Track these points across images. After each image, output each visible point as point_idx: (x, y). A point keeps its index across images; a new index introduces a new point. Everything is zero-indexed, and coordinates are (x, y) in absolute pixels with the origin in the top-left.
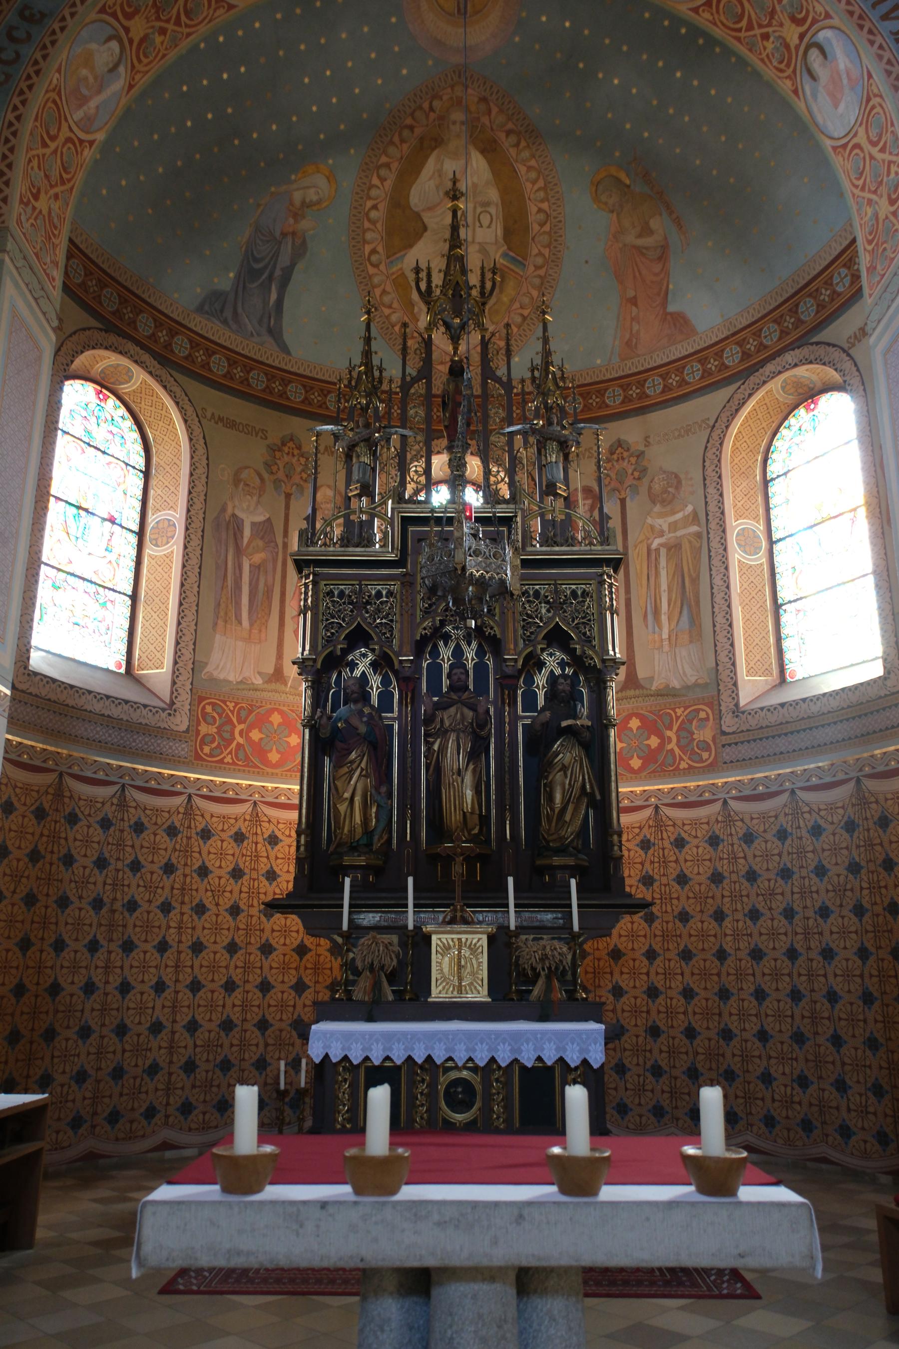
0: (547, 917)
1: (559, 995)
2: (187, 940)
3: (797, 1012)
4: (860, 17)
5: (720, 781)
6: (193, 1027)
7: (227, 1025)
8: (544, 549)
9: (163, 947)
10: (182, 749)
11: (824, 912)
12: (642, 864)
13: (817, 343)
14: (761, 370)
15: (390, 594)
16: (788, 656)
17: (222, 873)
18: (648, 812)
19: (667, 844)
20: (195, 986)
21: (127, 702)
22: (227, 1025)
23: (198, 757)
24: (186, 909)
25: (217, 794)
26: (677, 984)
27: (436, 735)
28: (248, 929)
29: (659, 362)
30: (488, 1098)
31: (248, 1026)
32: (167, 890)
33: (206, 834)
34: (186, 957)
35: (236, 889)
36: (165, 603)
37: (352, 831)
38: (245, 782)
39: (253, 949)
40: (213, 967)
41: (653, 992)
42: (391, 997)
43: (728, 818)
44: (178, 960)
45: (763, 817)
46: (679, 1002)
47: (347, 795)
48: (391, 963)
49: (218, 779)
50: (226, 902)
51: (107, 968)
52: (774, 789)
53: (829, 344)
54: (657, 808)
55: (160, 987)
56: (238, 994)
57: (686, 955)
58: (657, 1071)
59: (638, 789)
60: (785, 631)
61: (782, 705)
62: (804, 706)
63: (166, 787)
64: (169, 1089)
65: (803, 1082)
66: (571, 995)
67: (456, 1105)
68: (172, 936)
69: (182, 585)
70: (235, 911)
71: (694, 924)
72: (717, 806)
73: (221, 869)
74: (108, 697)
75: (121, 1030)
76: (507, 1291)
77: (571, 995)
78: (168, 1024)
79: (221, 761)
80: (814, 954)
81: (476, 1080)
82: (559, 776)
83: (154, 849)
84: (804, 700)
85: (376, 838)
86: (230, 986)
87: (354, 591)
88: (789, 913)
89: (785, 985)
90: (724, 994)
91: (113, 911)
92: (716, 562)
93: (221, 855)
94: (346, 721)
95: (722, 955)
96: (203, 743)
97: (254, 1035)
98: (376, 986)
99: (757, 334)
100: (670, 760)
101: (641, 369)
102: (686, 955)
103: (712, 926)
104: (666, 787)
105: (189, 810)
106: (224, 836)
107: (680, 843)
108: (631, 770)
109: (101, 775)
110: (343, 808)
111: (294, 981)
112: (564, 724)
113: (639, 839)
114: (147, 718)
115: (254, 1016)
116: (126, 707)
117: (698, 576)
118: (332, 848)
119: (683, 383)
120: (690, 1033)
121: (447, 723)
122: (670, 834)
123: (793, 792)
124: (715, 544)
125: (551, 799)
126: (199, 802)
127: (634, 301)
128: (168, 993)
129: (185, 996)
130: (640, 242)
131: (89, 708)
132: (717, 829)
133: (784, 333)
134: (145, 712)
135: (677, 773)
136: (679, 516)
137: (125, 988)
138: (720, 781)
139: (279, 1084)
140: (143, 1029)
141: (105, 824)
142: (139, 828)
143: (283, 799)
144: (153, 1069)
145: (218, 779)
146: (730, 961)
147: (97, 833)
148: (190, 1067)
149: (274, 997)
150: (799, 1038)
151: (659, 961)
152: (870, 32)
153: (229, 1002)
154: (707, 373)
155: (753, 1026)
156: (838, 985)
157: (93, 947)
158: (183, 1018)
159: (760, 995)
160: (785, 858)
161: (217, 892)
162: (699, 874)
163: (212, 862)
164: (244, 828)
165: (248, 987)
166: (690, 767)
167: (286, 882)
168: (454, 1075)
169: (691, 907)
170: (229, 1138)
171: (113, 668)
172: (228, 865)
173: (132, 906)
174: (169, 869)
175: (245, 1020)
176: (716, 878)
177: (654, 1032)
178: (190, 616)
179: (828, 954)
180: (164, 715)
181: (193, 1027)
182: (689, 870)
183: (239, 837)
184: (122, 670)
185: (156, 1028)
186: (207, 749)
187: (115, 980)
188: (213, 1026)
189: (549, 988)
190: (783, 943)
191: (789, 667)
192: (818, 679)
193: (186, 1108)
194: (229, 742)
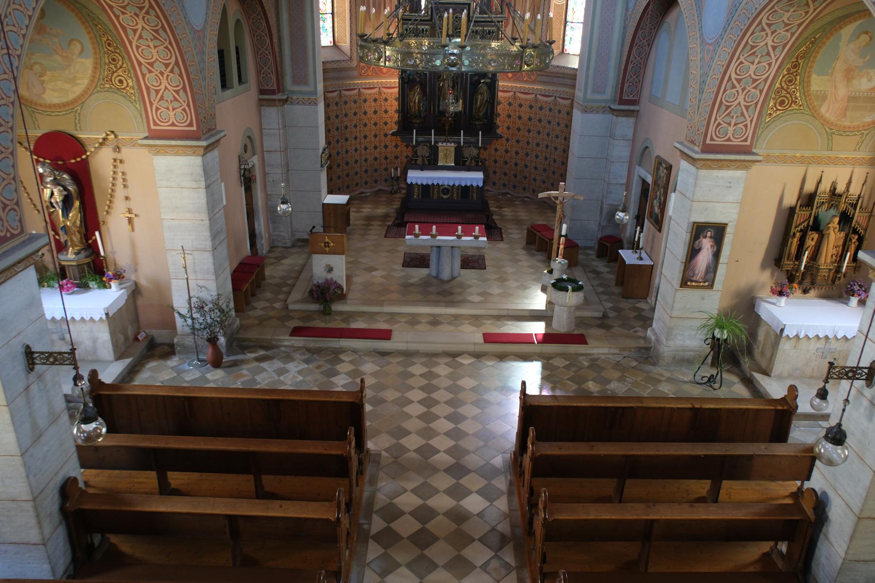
0: (473, 140)
1: (474, 164)
2: (362, 135)
3: (546, 163)
5: (535, 87)
6: (366, 160)
7: (376, 159)
8: (480, 16)
9: (356, 138)
10: (355, 73)
11: (557, 137)
12: (508, 110)
15: (426, 31)
16: (566, 43)
17: (370, 112)
18: (512, 94)
19: (516, 105)
20: (366, 149)
21: (338, 61)
22: (376, 159)
23: (361, 75)
24: (361, 126)
25: (367, 87)
26: (514, 150)
27: (441, 81)
28: (380, 130)
30: (453, 192)
31: (382, 159)
32: (355, 121)
33: (365, 101)
34: (363, 140)
35: (375, 117)
36: (345, 17)
37: (415, 111)
38: (375, 81)
39: (382, 135)
40: (370, 142)
41: (507, 151)
42: (427, 163)
43: (536, 100)
44: (360, 142)
45: (546, 102)
46: (514, 155)
47: (413, 101)
48: (427, 155)
49: (367, 81)
50: (373, 122)
51: (342, 147)
52: (551, 94)
54: (515, 92)
55: (356, 150)
56: (378, 149)
57: (518, 141)
58: (505, 174)
59: (510, 85)
60: (566, 33)
61: (558, 66)
62: (563, 69)
63: (352, 87)
64: (361, 178)
65: (544, 182)
66: (477, 165)
67: (444, 194)
68: (358, 135)
69: (350, 10)
70: (375, 124)
71: (521, 132)
72: (534, 95)
73: (370, 111)
74: (333, 61)
75: (347, 164)
76: (450, 248)
77: (477, 165)
78: (359, 160)
79: (368, 75)
80: (553, 148)
81: (450, 188)
82: (479, 96)
83: (351, 109)
84: (564, 67)
85: (422, 114)
86: (376, 147)
87: (413, 28)
88: (548, 135)
89: (544, 155)
90: (527, 155)
91: (342, 130)
93: (370, 107)
94: (413, 76)
95: (528, 143)
96: (362, 70)
97: (383, 161)
98: (423, 160)
100: (521, 76)
102: (518, 141)
103: (526, 134)
104: (519, 86)
105: (360, 93)
106: (371, 100)
107: (520, 106)
108: (508, 77)
109: (334, 89)
110: (412, 104)
111: (395, 144)
112: (482, 81)
113: (508, 102)
114: (344, 65)
115: (383, 156)
116: (338, 63)
118: (409, 116)
120: (516, 164)
121: (445, 77)
122: (518, 102)
123: (555, 97)
125: (476, 104)
126: (362, 90)
128: (358, 152)
129: (363, 151)
131: (328, 67)
132: (532, 103)
134: (344, 63)
135: (523, 81)
137: (347, 152)
138: (535, 87)
139: (391, 175)
140: (353, 163)
141: (337, 104)
142: (346, 103)
143: (388, 85)
144: (357, 173)
145: (367, 81)
146: (530, 145)
147: (335, 108)
148: (366, 171)
149: (389, 150)
150: (545, 170)
151: (510, 142)
153: (376, 152)
155: (533, 165)
156: (557, 159)
157: (338, 141)
158: (363, 158)
159: (537, 156)
160: (550, 118)
161: (370, 119)
162: (525, 117)
163: (368, 110)
164: (376, 96)
165: (381, 147)
166: (527, 80)
167: (395, 128)
168: (444, 187)
169: (521, 127)
170: (415, 230)
171: (330, 45)
172: (372, 110)
173: (346, 127)
174: (355, 114)
175: (381, 157)
176: (530, 119)
177: (506, 163)
178: (354, 22)
179: (556, 149)
180: (349, 62)
181: (366, 160)
182: (522, 115)
183: (375, 100)
184: (332, 44)
185: (356, 162)
186: (363, 71)
187: (344, 150)
188: (372, 159)
189: (471, 163)
190: (545, 143)
191: (565, 47)
192: (571, 57)
193: (366, 183)
194: (370, 68)
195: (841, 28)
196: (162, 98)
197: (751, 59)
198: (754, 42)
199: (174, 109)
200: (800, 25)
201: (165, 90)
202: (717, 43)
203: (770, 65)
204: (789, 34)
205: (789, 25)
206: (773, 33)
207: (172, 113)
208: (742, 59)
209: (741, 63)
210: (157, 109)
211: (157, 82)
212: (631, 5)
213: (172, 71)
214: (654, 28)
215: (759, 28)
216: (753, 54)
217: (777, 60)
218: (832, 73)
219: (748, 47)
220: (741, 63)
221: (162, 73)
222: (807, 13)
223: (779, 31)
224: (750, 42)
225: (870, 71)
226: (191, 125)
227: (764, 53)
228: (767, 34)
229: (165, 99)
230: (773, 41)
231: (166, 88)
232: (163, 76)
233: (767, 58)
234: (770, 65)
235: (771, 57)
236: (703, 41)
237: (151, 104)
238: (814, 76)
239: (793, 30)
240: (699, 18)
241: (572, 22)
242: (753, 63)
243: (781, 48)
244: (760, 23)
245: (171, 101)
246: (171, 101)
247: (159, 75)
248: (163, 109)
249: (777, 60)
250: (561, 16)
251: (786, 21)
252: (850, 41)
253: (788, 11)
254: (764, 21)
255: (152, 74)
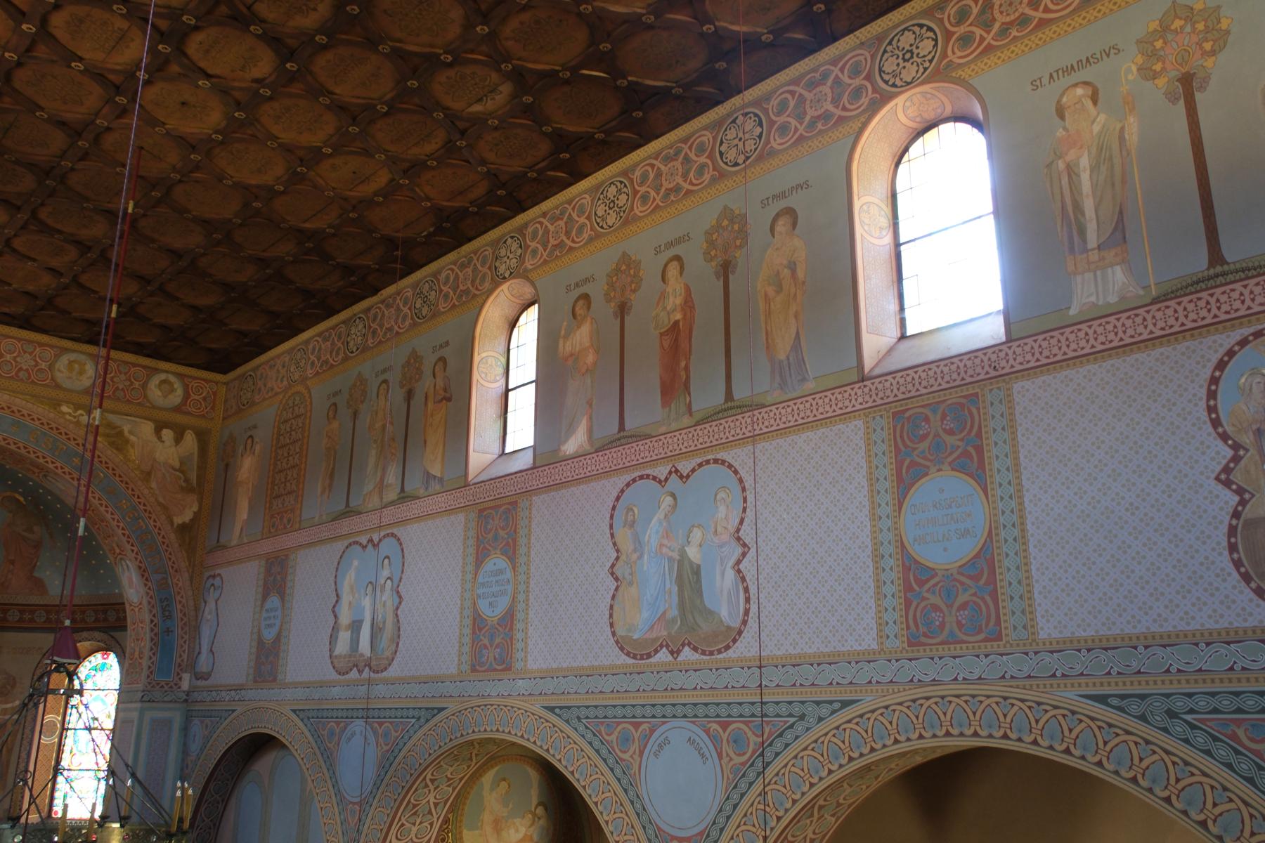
4: (144, 571)
13: (112, 637)
14: (80, 633)
29: (20, 602)
53: (118, 642)
92: (25, 742)
99: (83, 612)
101: (7, 602)
117: (12, 749)
119: (32, 620)
124: (27, 731)
127: (12, 562)
130: (25, 534)
133: (97, 620)
136: (9, 706)
152: (147, 580)
154: (48, 620)
195: (481, 776)
197: (411, 820)
198: (416, 801)
200: (461, 779)
202: (364, 804)
203: (431, 824)
204: (450, 789)
205: (452, 779)
206: (435, 789)
208: (403, 820)
209: (403, 825)
212: (194, 747)
214: (233, 778)
215: (423, 784)
216: (415, 814)
217: (438, 818)
218: (482, 826)
219: (411, 806)
220: (403, 825)
222: (469, 767)
223: (441, 787)
224: (412, 801)
225: (515, 820)
227: (426, 812)
228: (430, 790)
230: (435, 798)
233: (429, 816)
234: (431, 824)
235: (432, 815)
236: (342, 800)
238: (465, 832)
239: (455, 785)
240: (331, 772)
241: (68, 770)
242: (414, 824)
243: (442, 804)
244: (425, 779)
249: (438, 818)
250: (50, 761)
251: (449, 776)
252: (492, 790)
253: (452, 766)
254: (429, 776)
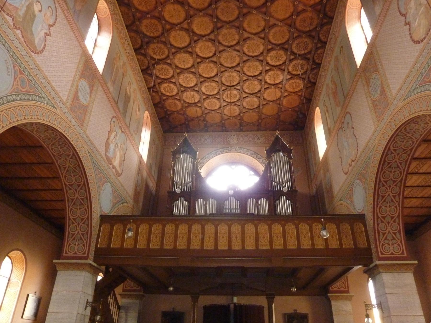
196: (386, 238)
199: (392, 244)
201: (388, 234)
207: (391, 247)
210: (383, 245)
211: (385, 228)
213: (394, 222)
221: (388, 223)
226: (403, 253)
229: (388, 238)
231: (389, 232)
232: (389, 224)
237: (380, 242)
245: (391, 240)
246: (391, 240)
247: (387, 224)
248: (386, 245)
255: (383, 224)
